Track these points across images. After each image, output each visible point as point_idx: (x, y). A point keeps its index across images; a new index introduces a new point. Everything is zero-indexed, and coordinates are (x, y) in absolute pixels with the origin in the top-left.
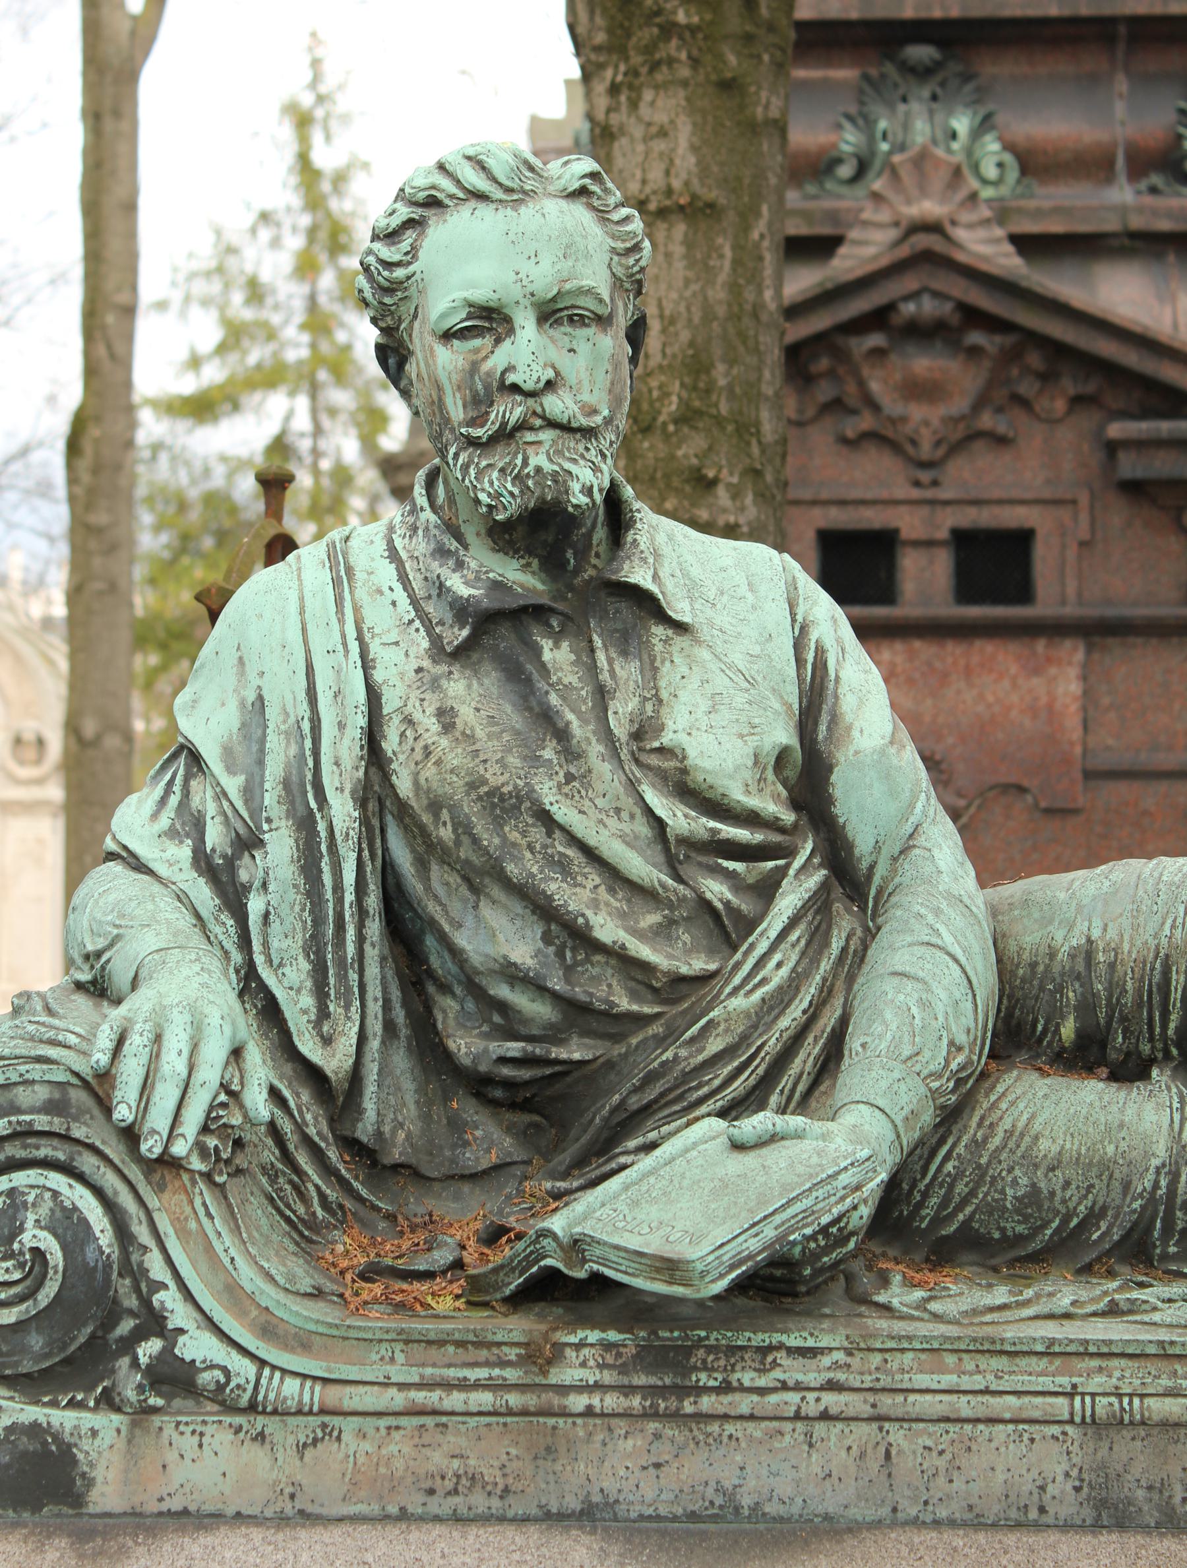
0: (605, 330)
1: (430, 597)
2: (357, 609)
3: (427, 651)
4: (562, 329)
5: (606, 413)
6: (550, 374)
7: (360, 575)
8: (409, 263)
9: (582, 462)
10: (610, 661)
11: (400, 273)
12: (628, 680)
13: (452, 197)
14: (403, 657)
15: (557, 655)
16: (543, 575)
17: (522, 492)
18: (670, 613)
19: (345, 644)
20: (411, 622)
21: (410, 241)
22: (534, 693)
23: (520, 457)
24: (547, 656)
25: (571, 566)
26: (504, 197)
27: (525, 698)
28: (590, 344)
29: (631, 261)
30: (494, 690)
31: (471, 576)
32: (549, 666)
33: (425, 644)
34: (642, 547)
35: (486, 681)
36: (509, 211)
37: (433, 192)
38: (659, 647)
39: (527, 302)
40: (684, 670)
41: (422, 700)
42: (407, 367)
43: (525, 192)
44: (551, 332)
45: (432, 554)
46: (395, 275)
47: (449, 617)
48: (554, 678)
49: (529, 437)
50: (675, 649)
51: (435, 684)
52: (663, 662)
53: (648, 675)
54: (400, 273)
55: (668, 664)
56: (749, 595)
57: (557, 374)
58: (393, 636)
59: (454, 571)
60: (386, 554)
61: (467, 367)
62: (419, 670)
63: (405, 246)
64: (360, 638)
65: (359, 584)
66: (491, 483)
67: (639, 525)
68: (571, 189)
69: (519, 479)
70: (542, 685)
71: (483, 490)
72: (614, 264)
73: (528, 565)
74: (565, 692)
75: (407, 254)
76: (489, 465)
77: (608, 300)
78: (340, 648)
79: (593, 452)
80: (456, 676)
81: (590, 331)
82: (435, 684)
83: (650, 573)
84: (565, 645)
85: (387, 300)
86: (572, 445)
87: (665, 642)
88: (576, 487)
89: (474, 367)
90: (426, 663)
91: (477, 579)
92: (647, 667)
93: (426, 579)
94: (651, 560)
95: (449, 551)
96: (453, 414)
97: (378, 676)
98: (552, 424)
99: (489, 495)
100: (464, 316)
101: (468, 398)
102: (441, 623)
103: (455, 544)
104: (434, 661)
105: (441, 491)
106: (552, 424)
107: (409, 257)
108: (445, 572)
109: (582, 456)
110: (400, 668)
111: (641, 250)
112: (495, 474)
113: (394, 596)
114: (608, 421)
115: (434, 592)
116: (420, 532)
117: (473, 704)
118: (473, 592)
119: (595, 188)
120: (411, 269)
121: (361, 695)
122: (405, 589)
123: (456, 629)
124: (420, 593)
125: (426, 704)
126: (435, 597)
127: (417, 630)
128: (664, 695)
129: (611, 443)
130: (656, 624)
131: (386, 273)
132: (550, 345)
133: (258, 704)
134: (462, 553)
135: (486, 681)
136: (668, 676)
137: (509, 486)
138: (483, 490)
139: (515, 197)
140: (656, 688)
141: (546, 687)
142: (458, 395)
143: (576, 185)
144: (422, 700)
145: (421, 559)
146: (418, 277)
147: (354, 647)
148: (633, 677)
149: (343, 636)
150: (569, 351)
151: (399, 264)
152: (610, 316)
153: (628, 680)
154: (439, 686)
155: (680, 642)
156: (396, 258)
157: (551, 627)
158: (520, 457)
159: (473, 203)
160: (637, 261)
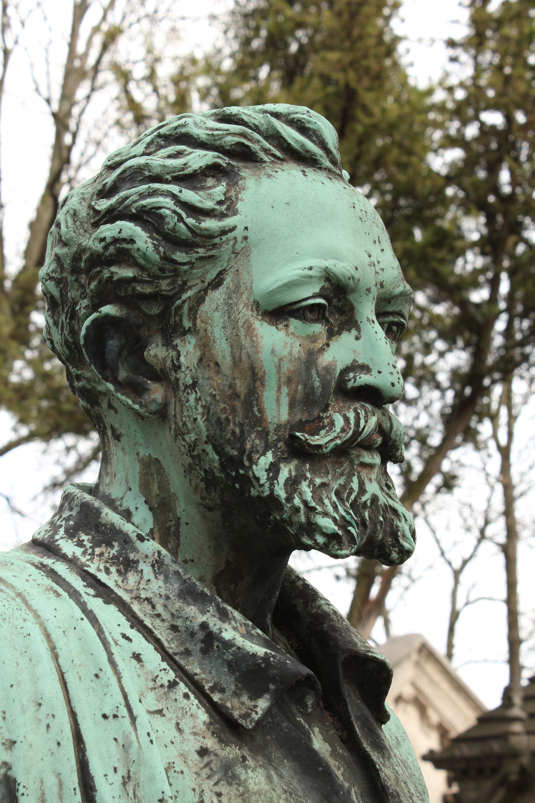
3: (208, 725)
8: (222, 216)
11: (210, 224)
14: (177, 734)
20: (172, 685)
22: (337, 793)
23: (355, 479)
33: (203, 716)
46: (204, 225)
47: (229, 682)
54: (210, 224)
61: (304, 356)
62: (203, 752)
78: (123, 711)
85: (180, 256)
89: (310, 359)
90: (210, 743)
100: (317, 290)
102: (217, 688)
115: (196, 648)
120: (229, 222)
123: (245, 698)
124: (172, 647)
131: (191, 221)
138: (326, 514)
142: (285, 390)
154: (235, 777)
156: (209, 204)
158: (355, 479)
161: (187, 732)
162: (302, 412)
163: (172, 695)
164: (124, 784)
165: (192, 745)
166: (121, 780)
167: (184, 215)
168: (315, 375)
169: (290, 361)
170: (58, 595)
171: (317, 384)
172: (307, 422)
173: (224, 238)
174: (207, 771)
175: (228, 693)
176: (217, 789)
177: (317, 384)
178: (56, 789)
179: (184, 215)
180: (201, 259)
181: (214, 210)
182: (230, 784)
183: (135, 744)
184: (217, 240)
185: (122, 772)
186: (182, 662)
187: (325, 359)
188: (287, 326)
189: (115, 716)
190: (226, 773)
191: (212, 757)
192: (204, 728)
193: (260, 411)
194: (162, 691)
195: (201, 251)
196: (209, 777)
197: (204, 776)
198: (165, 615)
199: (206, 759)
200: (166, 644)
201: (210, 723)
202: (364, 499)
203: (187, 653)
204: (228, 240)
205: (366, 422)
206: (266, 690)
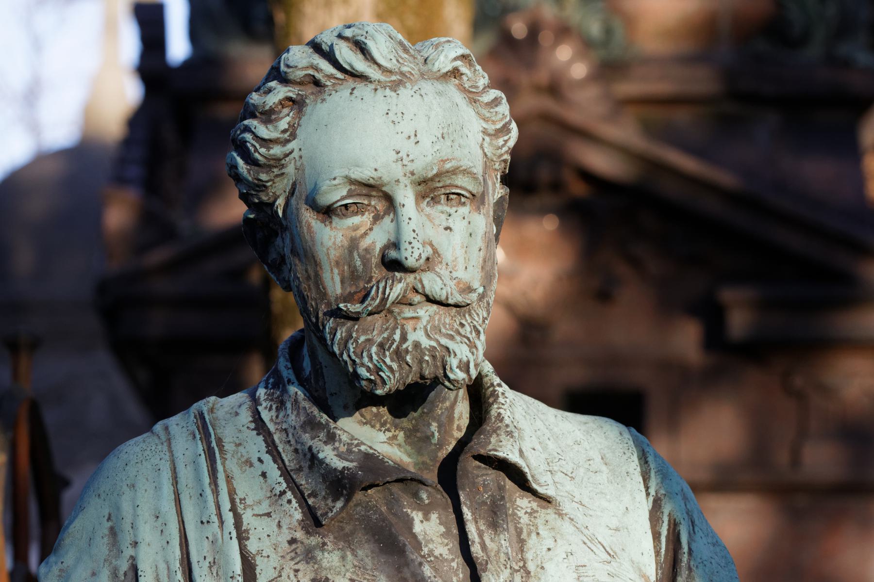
0: (478, 209)
1: (300, 469)
2: (229, 479)
3: (300, 522)
4: (440, 207)
5: (481, 290)
6: (429, 251)
7: (229, 447)
8: (287, 141)
9: (458, 338)
10: (481, 536)
12: (498, 552)
13: (330, 77)
14: (276, 529)
15: (430, 529)
16: (408, 448)
17: (400, 366)
18: (535, 486)
19: (220, 515)
20: (283, 493)
21: (288, 119)
22: (407, 565)
23: (398, 332)
24: (418, 528)
25: (435, 440)
26: (383, 78)
27: (399, 570)
28: (465, 222)
29: (501, 142)
30: (368, 562)
31: (343, 449)
32: (420, 538)
33: (298, 515)
34: (507, 421)
35: (360, 553)
36: (388, 92)
37: (311, 72)
38: (524, 519)
39: (405, 181)
40: (549, 543)
41: (297, 571)
42: (279, 241)
43: (402, 74)
44: (428, 210)
45: (302, 427)
46: (272, 152)
48: (425, 550)
49: (408, 312)
50: (540, 522)
51: (309, 556)
52: (529, 534)
53: (516, 546)
55: (534, 536)
56: (604, 468)
57: (435, 251)
58: (264, 508)
59: (326, 443)
60: (253, 426)
61: (346, 243)
62: (292, 541)
63: (283, 124)
64: (233, 509)
65: (228, 456)
66: (371, 358)
67: (501, 400)
68: (444, 70)
69: (399, 355)
70: (413, 556)
71: (363, 365)
72: (486, 145)
73: (395, 437)
74: (437, 562)
75: (284, 131)
76: (368, 340)
77: (481, 179)
78: (215, 518)
79: (468, 328)
80: (330, 546)
81: (464, 210)
82: (309, 556)
83: (517, 448)
84: (434, 516)
85: (264, 177)
86: (448, 321)
87: (530, 514)
88: (454, 362)
90: (299, 535)
91: (349, 451)
92: (515, 539)
93: (296, 451)
94: (516, 434)
95: (320, 423)
96: (330, 291)
97: (252, 546)
98: (430, 300)
99: (369, 370)
100: (344, 193)
101: (347, 274)
102: (313, 494)
103: (325, 416)
104: (308, 533)
105: (307, 364)
106: (430, 300)
107: (286, 135)
108: (317, 444)
109: (459, 333)
110: (273, 539)
111: (509, 131)
112: (374, 349)
113: (263, 468)
114: (482, 297)
115: (306, 464)
116: (289, 405)
117: (348, 575)
118: (346, 464)
119: (464, 70)
121: (237, 566)
122: (275, 461)
123: (329, 502)
124: (290, 464)
125: (300, 574)
126: (306, 470)
127: (289, 502)
128: (531, 566)
129: (484, 319)
130: (522, 497)
131: (263, 150)
132: (428, 224)
133: (131, 575)
134: (332, 425)
135: (360, 553)
136: (535, 548)
137: (388, 360)
138: (363, 365)
139: (394, 78)
140: (523, 560)
141: (419, 559)
142: (336, 271)
143: (449, 67)
144: (297, 571)
145: (291, 431)
146: (295, 154)
147: (229, 518)
148: (504, 549)
149: (218, 507)
150: (446, 229)
151: (275, 141)
152: (483, 195)
153: (498, 552)
154: (313, 558)
155: (549, 514)
156: (274, 135)
157: (421, 499)
158: (398, 332)
159: (351, 82)
160: (506, 141)
161: (285, 527)
162: (351, 286)
163: (280, 502)
164: (210, 567)
165: (286, 535)
166: (208, 565)
167: (258, 146)
168: (356, 257)
169: (335, 249)
170: (194, 437)
171: (358, 263)
172: (355, 293)
173: (287, 159)
174: (293, 554)
175: (320, 497)
176: (296, 567)
177: (358, 263)
178: (166, 572)
179: (258, 146)
180: (277, 176)
181: (278, 138)
182: (308, 563)
183: (220, 540)
184: (283, 162)
185: (210, 559)
186: (294, 477)
187: (365, 243)
188: (331, 222)
189: (208, 522)
190: (307, 555)
191: (299, 545)
192: (296, 524)
193: (324, 289)
194: (274, 498)
195: (276, 171)
196: (292, 559)
197: (288, 557)
198: (293, 442)
199: (294, 546)
200: (287, 463)
201: (303, 520)
202: (404, 346)
203: (300, 469)
204: (291, 160)
205: (391, 289)
206: (342, 495)
